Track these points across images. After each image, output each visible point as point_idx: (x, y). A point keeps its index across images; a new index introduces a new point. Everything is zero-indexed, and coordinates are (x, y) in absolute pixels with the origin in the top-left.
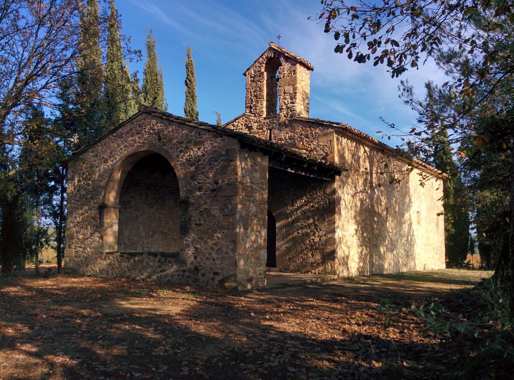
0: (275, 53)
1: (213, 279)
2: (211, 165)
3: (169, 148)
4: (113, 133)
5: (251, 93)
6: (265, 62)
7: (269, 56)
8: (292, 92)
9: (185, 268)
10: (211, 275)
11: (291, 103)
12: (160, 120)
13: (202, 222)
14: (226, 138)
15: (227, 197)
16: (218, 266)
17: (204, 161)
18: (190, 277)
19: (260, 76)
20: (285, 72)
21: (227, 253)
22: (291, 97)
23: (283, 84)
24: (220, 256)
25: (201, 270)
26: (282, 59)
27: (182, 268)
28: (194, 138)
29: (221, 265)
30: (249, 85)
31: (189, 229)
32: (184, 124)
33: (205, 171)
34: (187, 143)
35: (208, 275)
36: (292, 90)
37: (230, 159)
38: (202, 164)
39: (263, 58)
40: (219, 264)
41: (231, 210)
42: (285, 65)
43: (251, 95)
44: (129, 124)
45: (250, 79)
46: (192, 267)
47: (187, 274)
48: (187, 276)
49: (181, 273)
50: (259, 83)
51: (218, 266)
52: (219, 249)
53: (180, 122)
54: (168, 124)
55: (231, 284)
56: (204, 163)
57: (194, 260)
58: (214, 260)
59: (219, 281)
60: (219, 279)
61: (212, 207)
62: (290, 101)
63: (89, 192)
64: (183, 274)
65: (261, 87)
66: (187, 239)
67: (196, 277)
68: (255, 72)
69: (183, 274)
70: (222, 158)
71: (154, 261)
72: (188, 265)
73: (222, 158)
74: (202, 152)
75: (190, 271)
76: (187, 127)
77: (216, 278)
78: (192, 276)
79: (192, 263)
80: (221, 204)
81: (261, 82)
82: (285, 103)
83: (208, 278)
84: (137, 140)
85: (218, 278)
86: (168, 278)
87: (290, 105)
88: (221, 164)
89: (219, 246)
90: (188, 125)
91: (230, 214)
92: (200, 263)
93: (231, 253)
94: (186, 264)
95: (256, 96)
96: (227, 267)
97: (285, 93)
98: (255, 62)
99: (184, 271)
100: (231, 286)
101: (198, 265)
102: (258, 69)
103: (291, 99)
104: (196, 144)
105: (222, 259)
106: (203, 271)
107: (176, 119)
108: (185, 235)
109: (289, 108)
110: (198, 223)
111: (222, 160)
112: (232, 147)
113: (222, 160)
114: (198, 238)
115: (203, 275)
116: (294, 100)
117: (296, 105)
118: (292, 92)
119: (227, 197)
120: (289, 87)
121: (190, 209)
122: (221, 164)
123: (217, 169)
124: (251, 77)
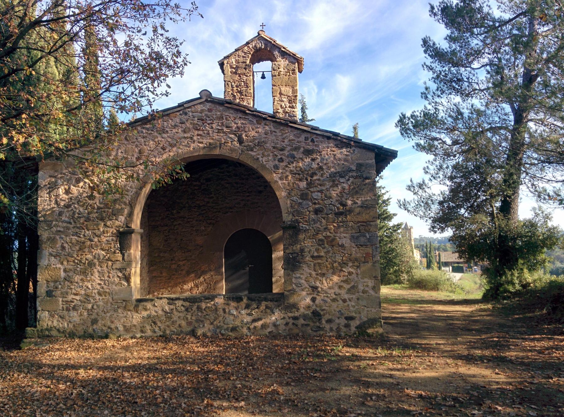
0: (265, 45)
1: (347, 326)
2: (334, 181)
3: (258, 154)
4: (146, 124)
5: (232, 87)
6: (252, 53)
7: (258, 46)
8: (290, 94)
9: (297, 314)
10: (343, 321)
11: (290, 107)
12: (240, 115)
13: (322, 254)
14: (357, 150)
15: (361, 222)
16: (352, 309)
17: (322, 176)
18: (307, 325)
19: (245, 69)
20: (282, 69)
21: (364, 292)
22: (290, 100)
23: (279, 83)
24: (354, 296)
25: (324, 315)
26: (276, 53)
27: (290, 315)
28: (303, 144)
29: (357, 307)
30: (229, 77)
31: (299, 262)
32: (287, 125)
33: (324, 188)
34: (291, 150)
35: (337, 321)
36: (291, 93)
37: (364, 176)
38: (319, 180)
39: (248, 47)
40: (354, 307)
41: (369, 239)
42: (280, 61)
43: (232, 90)
44: (178, 114)
45: (230, 70)
46: (309, 312)
47: (301, 321)
48: (302, 325)
49: (291, 321)
50: (245, 78)
51: (352, 309)
52: (353, 287)
53: (272, 119)
54: (255, 122)
55: (376, 330)
56: (322, 179)
57: (312, 303)
58: (344, 301)
59: (356, 327)
60: (355, 325)
61: (338, 235)
62: (288, 105)
63: (94, 208)
64: (295, 322)
65: (248, 82)
66: (298, 275)
67: (318, 324)
68: (237, 62)
69: (295, 322)
70: (351, 174)
71: (237, 308)
72: (302, 310)
73: (351, 174)
74: (318, 164)
75: (305, 317)
76: (290, 129)
77: (352, 324)
78: (312, 324)
79: (309, 307)
80: (354, 231)
81: (247, 76)
82: (281, 106)
83: (339, 324)
84: (195, 138)
85: (354, 324)
86: (269, 330)
87: (288, 110)
88: (351, 181)
89: (352, 284)
90: (292, 127)
91: (368, 243)
92: (320, 307)
93: (372, 292)
94: (298, 309)
95: (240, 92)
96: (366, 309)
97: (281, 94)
98: (236, 50)
99: (295, 318)
100: (377, 332)
101: (318, 309)
102: (241, 59)
103: (289, 103)
104: (308, 152)
105: (358, 299)
106: (327, 317)
107: (269, 116)
108: (293, 271)
109: (287, 112)
110: (316, 254)
111: (352, 177)
112: (367, 161)
113: (352, 177)
114: (317, 274)
115: (329, 321)
116: (294, 105)
117: (295, 110)
118: (290, 94)
119: (361, 222)
120: (288, 89)
121: (301, 236)
122: (351, 181)
123: (344, 189)
124: (231, 67)
